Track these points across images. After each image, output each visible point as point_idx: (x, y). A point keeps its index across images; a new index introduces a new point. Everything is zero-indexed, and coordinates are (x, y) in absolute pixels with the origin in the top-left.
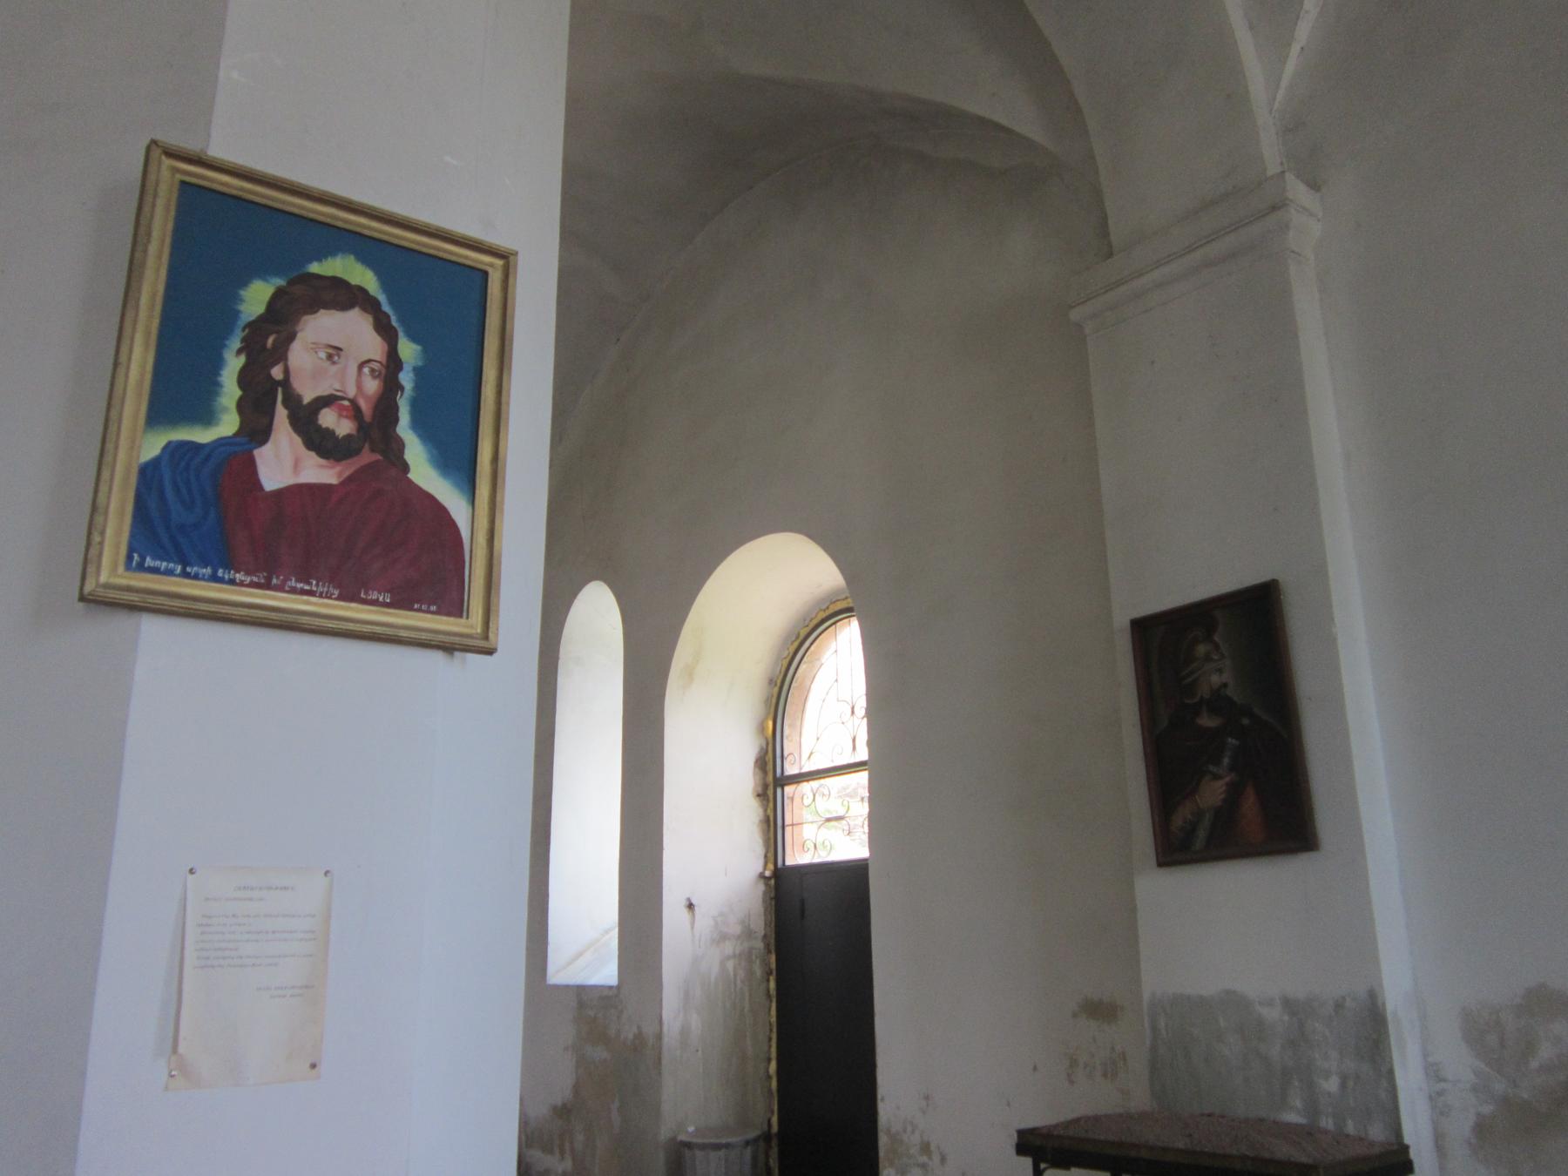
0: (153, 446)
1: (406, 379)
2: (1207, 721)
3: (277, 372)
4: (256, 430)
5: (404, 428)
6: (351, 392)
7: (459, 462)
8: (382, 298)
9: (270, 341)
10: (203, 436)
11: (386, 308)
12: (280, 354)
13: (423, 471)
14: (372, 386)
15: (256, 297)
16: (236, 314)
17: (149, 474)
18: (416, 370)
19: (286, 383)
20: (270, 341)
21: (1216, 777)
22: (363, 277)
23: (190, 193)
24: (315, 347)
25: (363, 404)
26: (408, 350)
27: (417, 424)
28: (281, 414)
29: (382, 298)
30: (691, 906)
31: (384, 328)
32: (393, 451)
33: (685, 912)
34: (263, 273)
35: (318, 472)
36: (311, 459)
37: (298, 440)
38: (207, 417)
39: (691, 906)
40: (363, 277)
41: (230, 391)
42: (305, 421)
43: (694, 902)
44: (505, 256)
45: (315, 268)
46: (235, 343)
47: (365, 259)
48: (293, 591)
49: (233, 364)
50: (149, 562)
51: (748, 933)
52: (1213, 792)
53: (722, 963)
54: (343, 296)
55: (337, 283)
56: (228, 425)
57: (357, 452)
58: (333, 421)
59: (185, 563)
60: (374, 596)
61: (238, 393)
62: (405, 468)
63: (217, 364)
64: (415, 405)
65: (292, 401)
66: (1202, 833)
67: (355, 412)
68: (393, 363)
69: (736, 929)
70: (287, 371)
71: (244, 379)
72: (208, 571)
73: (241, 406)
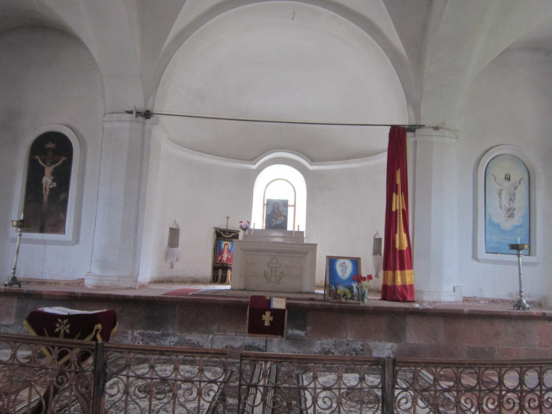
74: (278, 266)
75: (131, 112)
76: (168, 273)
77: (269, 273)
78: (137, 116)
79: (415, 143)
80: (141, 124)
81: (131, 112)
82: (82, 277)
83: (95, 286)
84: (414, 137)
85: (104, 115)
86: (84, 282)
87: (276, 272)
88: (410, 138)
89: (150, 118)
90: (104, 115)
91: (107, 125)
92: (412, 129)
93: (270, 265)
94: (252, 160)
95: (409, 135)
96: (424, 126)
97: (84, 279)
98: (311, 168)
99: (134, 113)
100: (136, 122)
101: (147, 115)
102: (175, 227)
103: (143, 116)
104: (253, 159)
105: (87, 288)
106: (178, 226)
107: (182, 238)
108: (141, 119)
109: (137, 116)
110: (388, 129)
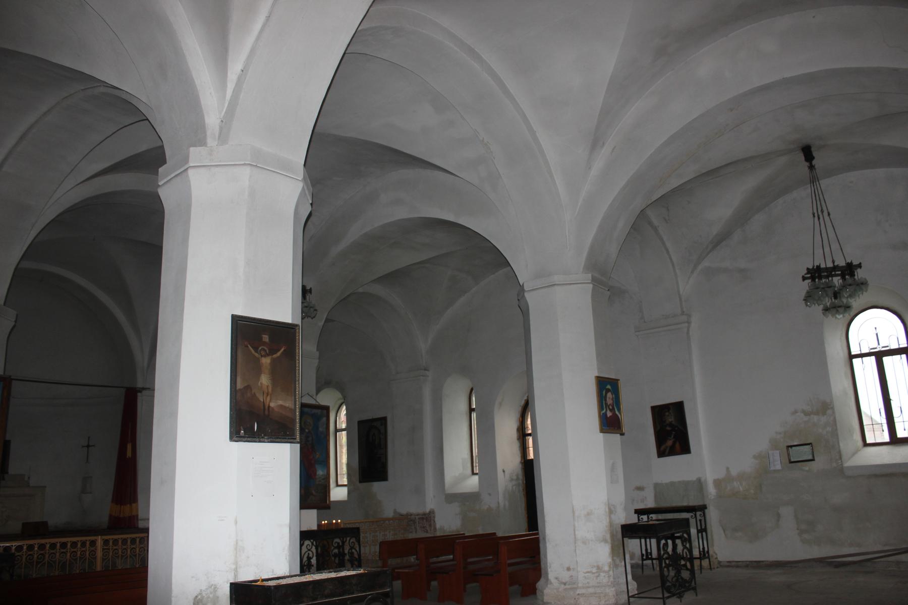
2: (668, 428)
4: (606, 410)
13: (617, 413)
21: (670, 440)
30: (504, 471)
31: (612, 394)
33: (502, 472)
38: (603, 409)
39: (504, 471)
43: (505, 470)
49: (604, 402)
51: (518, 479)
52: (670, 443)
53: (512, 487)
66: (667, 451)
69: (515, 477)
96: (149, 388)
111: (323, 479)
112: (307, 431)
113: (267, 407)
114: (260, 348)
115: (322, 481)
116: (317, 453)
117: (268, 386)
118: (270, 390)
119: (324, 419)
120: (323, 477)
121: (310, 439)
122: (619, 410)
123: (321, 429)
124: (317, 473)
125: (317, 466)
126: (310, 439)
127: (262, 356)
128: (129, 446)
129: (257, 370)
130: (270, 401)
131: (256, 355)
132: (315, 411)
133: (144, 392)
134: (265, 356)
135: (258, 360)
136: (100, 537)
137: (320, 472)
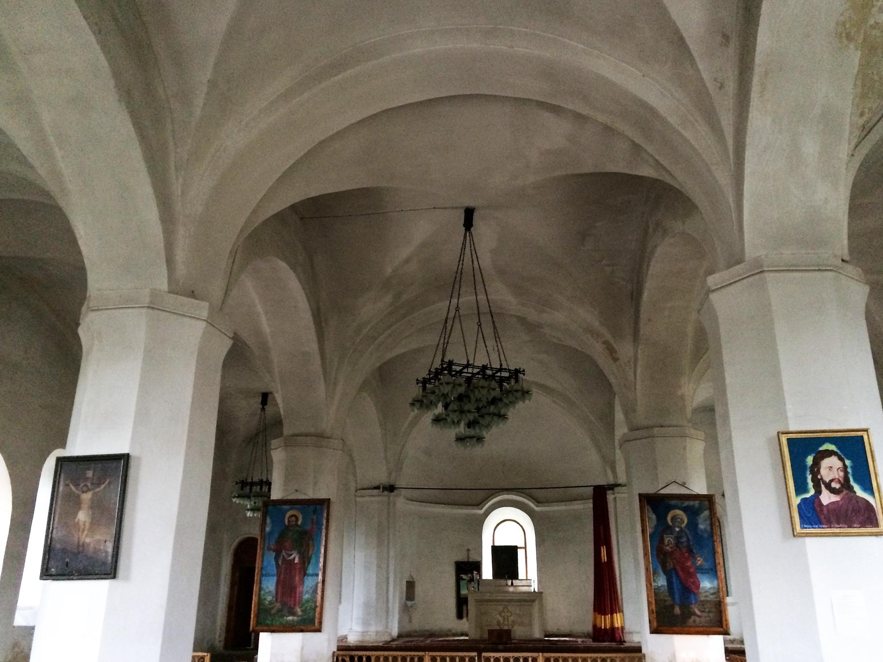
0: (796, 501)
1: (849, 470)
3: (819, 477)
4: (818, 492)
5: (852, 483)
6: (837, 477)
7: (869, 488)
8: (838, 451)
9: (816, 469)
10: (808, 496)
11: (840, 453)
12: (819, 472)
13: (860, 492)
14: (842, 474)
15: (810, 460)
16: (805, 466)
17: (799, 506)
18: (851, 467)
19: (822, 479)
20: (816, 469)
22: (832, 447)
23: (789, 441)
24: (826, 468)
25: (840, 479)
26: (848, 463)
27: (855, 480)
28: (823, 486)
29: (838, 451)
32: (851, 489)
34: (810, 454)
35: (835, 498)
36: (832, 495)
37: (828, 491)
38: (806, 490)
40: (832, 447)
41: (810, 484)
42: (828, 486)
44: (866, 430)
45: (821, 449)
46: (808, 472)
47: (831, 443)
48: (837, 528)
50: (805, 526)
54: (829, 453)
55: (827, 451)
56: (812, 492)
57: (843, 491)
58: (833, 485)
59: (812, 525)
60: (855, 526)
61: (812, 484)
62: (855, 492)
63: (806, 479)
64: (853, 475)
65: (825, 483)
67: (839, 482)
68: (845, 467)
70: (821, 476)
71: (813, 481)
72: (817, 526)
73: (814, 486)
74: (509, 614)
75: (377, 488)
76: (408, 628)
77: (502, 621)
78: (383, 491)
79: (615, 499)
80: (386, 498)
81: (377, 488)
82: (345, 634)
83: (357, 641)
84: (613, 494)
85: (356, 491)
86: (347, 638)
87: (508, 621)
88: (610, 497)
89: (393, 492)
90: (356, 491)
91: (358, 499)
92: (612, 487)
93: (503, 614)
94: (478, 505)
95: (609, 492)
96: (620, 484)
97: (347, 635)
98: (536, 509)
99: (381, 489)
100: (383, 496)
101: (391, 488)
102: (411, 580)
103: (387, 490)
104: (479, 504)
105: (350, 643)
106: (413, 579)
107: (419, 590)
108: (386, 493)
109: (383, 491)
110: (591, 489)
111: (712, 594)
112: (677, 529)
113: (81, 543)
114: (82, 485)
115: (711, 596)
116: (699, 559)
117: (85, 522)
118: (87, 526)
119: (706, 513)
120: (712, 591)
121: (684, 539)
122: (868, 487)
123: (702, 526)
124: (701, 586)
125: (699, 575)
126: (684, 539)
127: (83, 492)
128: (604, 551)
129: (77, 504)
130: (87, 536)
131: (77, 492)
132: (691, 503)
133: (617, 489)
134: (86, 492)
135: (79, 496)
136: (427, 653)
137: (706, 584)
